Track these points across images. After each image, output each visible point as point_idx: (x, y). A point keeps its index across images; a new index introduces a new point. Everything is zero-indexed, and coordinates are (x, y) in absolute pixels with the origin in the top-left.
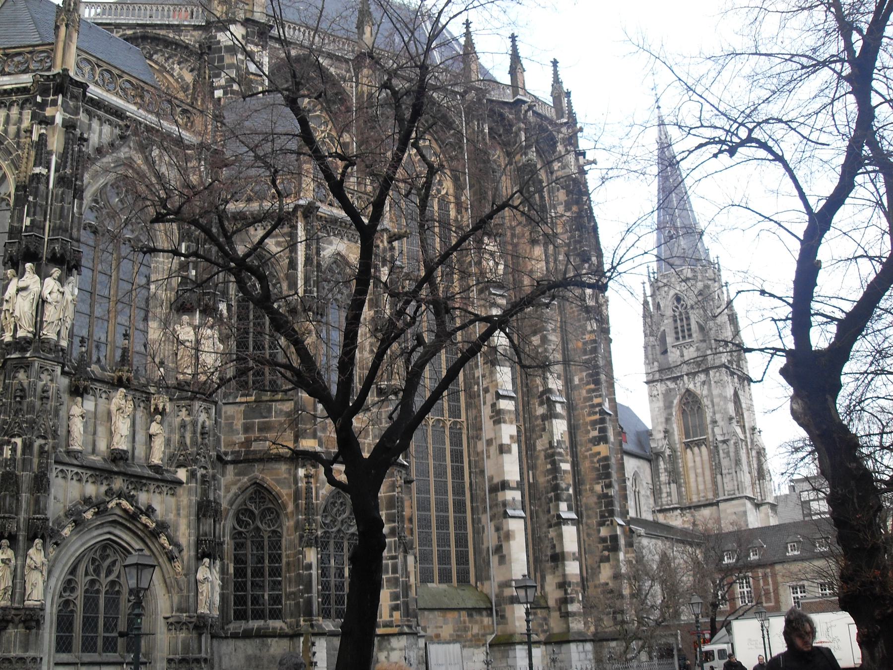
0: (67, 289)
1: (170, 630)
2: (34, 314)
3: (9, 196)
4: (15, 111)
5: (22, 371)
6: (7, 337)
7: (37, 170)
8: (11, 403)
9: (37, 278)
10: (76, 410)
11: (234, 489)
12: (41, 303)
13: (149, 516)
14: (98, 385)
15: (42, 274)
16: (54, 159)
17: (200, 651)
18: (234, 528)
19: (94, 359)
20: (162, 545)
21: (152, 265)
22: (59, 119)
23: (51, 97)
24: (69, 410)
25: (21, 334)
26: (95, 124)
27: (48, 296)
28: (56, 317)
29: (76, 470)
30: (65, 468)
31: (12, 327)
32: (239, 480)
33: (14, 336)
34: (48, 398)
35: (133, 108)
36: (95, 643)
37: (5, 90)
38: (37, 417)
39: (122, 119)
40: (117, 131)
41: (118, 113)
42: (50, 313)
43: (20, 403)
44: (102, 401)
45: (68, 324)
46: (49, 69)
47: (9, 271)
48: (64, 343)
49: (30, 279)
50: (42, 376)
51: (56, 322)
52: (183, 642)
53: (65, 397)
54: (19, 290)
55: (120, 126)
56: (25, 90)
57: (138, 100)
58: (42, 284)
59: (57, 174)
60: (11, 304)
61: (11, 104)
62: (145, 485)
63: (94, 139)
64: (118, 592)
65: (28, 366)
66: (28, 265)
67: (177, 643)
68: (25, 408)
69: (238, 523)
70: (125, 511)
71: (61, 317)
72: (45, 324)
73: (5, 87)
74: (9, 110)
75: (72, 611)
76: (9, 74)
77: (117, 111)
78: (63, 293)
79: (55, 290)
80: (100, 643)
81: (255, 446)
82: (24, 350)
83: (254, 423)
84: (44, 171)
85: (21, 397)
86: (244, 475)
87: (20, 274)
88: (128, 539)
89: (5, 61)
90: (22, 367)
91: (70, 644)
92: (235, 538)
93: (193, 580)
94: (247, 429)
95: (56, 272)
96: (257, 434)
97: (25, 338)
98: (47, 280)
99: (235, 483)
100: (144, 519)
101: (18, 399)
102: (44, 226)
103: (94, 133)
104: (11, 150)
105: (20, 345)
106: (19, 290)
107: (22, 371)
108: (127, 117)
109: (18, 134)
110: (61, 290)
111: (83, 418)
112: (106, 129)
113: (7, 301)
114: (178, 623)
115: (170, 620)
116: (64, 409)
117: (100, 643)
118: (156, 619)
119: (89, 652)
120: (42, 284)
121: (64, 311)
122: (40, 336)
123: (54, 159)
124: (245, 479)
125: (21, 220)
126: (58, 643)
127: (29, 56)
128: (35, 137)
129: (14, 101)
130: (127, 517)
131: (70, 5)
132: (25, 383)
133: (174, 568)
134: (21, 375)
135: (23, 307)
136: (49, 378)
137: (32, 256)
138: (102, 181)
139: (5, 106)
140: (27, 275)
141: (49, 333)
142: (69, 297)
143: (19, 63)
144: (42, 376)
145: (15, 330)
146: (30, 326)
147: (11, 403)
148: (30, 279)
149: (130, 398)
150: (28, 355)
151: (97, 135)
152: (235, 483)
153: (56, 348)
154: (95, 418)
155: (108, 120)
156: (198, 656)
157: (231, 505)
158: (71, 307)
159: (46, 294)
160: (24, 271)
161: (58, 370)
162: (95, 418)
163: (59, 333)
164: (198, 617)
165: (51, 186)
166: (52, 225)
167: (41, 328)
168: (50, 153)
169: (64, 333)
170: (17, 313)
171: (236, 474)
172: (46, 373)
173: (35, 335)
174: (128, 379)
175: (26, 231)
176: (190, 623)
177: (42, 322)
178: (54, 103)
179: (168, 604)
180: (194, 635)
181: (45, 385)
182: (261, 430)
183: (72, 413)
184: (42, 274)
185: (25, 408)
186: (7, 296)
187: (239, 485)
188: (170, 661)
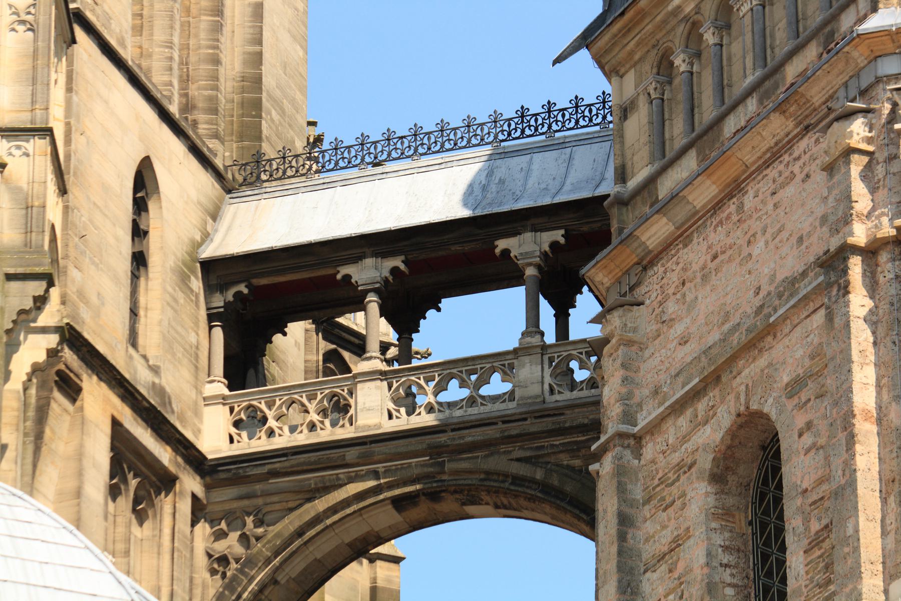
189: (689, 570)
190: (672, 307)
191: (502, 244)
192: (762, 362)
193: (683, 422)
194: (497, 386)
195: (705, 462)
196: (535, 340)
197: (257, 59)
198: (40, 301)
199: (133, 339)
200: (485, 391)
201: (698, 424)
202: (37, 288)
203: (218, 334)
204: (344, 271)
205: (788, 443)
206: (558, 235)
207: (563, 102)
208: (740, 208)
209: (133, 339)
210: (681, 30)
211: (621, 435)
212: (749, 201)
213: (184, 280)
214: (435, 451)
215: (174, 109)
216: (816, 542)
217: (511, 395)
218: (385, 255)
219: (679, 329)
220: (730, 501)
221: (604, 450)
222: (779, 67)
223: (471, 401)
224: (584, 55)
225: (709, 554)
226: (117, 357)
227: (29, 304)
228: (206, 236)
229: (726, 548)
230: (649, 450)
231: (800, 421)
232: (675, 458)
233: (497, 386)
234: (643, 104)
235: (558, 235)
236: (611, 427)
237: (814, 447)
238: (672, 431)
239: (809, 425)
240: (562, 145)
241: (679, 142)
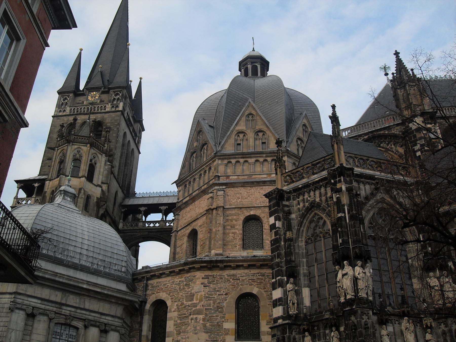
0: (367, 270)
2: (353, 286)
3: (329, 230)
4: (323, 190)
5: (353, 316)
6: (342, 300)
7: (339, 215)
8: (350, 333)
9: (351, 267)
10: (384, 332)
12: (355, 280)
14: (393, 317)
15: (353, 266)
16: (346, 207)
19: (388, 304)
21: (407, 249)
22: (344, 188)
23: (338, 179)
24: (380, 333)
25: (348, 297)
26: (362, 186)
27: (358, 276)
28: (364, 285)
31: (344, 294)
33: (345, 299)
34: (368, 328)
35: (378, 173)
37: (316, 181)
38: (365, 339)
39: (374, 180)
40: (373, 187)
41: (371, 177)
42: (361, 284)
43: (355, 332)
44: (397, 326)
45: (371, 288)
46: (334, 166)
47: (336, 267)
48: (371, 298)
49: (348, 269)
50: (363, 317)
51: (364, 288)
53: (377, 326)
54: (343, 275)
55: (373, 184)
56: (325, 179)
57: (379, 169)
58: (354, 270)
59: (349, 215)
60: (341, 283)
61: (321, 187)
63: (363, 193)
65: (355, 313)
66: (345, 262)
68: (358, 335)
71: (367, 285)
72: (359, 290)
73: (316, 180)
74: (320, 190)
76: (316, 173)
77: (370, 177)
78: (365, 273)
79: (361, 271)
82: (351, 305)
84: (343, 215)
85: (355, 329)
87: (342, 267)
89: (313, 168)
90: (352, 314)
95: (359, 263)
97: (351, 299)
98: (356, 268)
101: (353, 331)
102: (349, 241)
103: (362, 191)
104: (325, 208)
105: (349, 302)
106: (343, 275)
107: (353, 316)
108: (376, 178)
109: (326, 200)
110: (364, 271)
111: (388, 336)
112: (367, 187)
113: (339, 282)
116: (377, 332)
120: (354, 270)
121: (367, 281)
122: (358, 297)
123: (346, 207)
125: (337, 241)
127: (323, 162)
128: (335, 200)
129: (321, 185)
131: (336, 133)
132: (355, 321)
134: (353, 318)
135: (347, 283)
136: (367, 317)
137: (346, 257)
138: (371, 213)
139: (318, 189)
140: (345, 267)
141: (362, 294)
142: (368, 274)
143: (320, 167)
144: (363, 317)
145: (346, 296)
146: (352, 293)
147: (350, 333)
148: (348, 269)
149: (411, 321)
150: (354, 307)
151: (364, 191)
153: (367, 301)
154: (395, 335)
155: (367, 182)
158: (370, 279)
159: (357, 274)
160: (344, 265)
161: (371, 313)
162: (395, 335)
163: (367, 294)
165: (348, 221)
166: (352, 240)
167: (358, 293)
168: (344, 205)
169: (370, 293)
170: (344, 287)
172: (365, 315)
173: (355, 296)
174: (408, 312)
175: (340, 246)
177: (358, 289)
178: (340, 181)
181: (366, 321)
183: (382, 334)
184: (353, 266)
185: (358, 335)
186: (338, 280)
189: (183, 248)
190: (184, 215)
191: (160, 207)
192: (196, 222)
193: (184, 229)
194: (157, 225)
195: (187, 235)
196: (162, 220)
197: (130, 182)
198: (104, 205)
199: (113, 213)
200: (156, 225)
201: (186, 230)
202: (104, 203)
203: (122, 214)
204: (139, 208)
205: (199, 233)
206: (167, 207)
207: (169, 191)
208: (195, 204)
209: (113, 213)
210: (188, 182)
211: (175, 231)
212: (196, 203)
213: (119, 207)
214: (148, 232)
215: (121, 185)
216: (202, 245)
217: (159, 226)
218: (145, 207)
219: (185, 218)
220: (189, 240)
221: (173, 232)
222: (201, 187)
223: (154, 226)
224: (175, 184)
225: (186, 246)
226: (111, 214)
227: (103, 205)
228: (122, 202)
229: (189, 246)
230: (179, 233)
231: (201, 230)
232: (183, 234)
233: (157, 225)
234: (182, 190)
235: (167, 207)
236: (174, 229)
237: (202, 233)
238: (182, 231)
239: (202, 231)
240: (168, 196)
241: (186, 196)
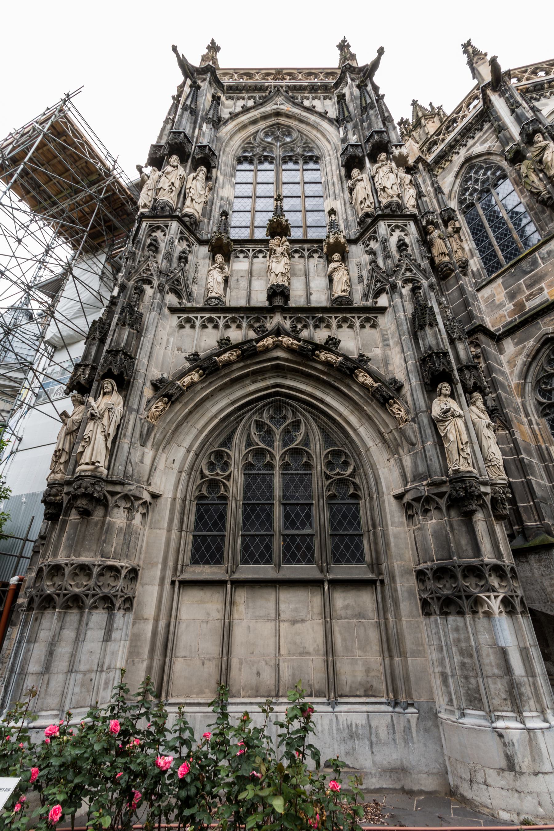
1: (410, 517)
11: (521, 360)
13: (331, 351)
17: (477, 551)
18: (540, 403)
20: (363, 386)
29: (208, 315)
30: (191, 316)
32: (525, 346)
36: (269, 548)
52: (435, 535)
62: (322, 320)
64: (308, 466)
67: (425, 538)
69: (544, 396)
70: (289, 349)
75: (224, 498)
80: (277, 544)
81: (529, 305)
83: (521, 283)
86: (527, 339)
88: (309, 389)
91: (220, 549)
92: (546, 415)
93: (425, 420)
94: (512, 296)
96: (527, 293)
99: (519, 353)
100: (323, 356)
114: (417, 499)
115: (408, 498)
117: (277, 544)
118: (381, 504)
119: (257, 562)
124: (531, 342)
126: (196, 548)
130: (299, 359)
133: (392, 416)
152: (519, 353)
156: (475, 561)
157: (525, 378)
164: (451, 481)
171: (516, 344)
176: (441, 495)
179: (396, 473)
180: (455, 517)
182: (529, 287)
187: (525, 352)
188: (421, 575)
